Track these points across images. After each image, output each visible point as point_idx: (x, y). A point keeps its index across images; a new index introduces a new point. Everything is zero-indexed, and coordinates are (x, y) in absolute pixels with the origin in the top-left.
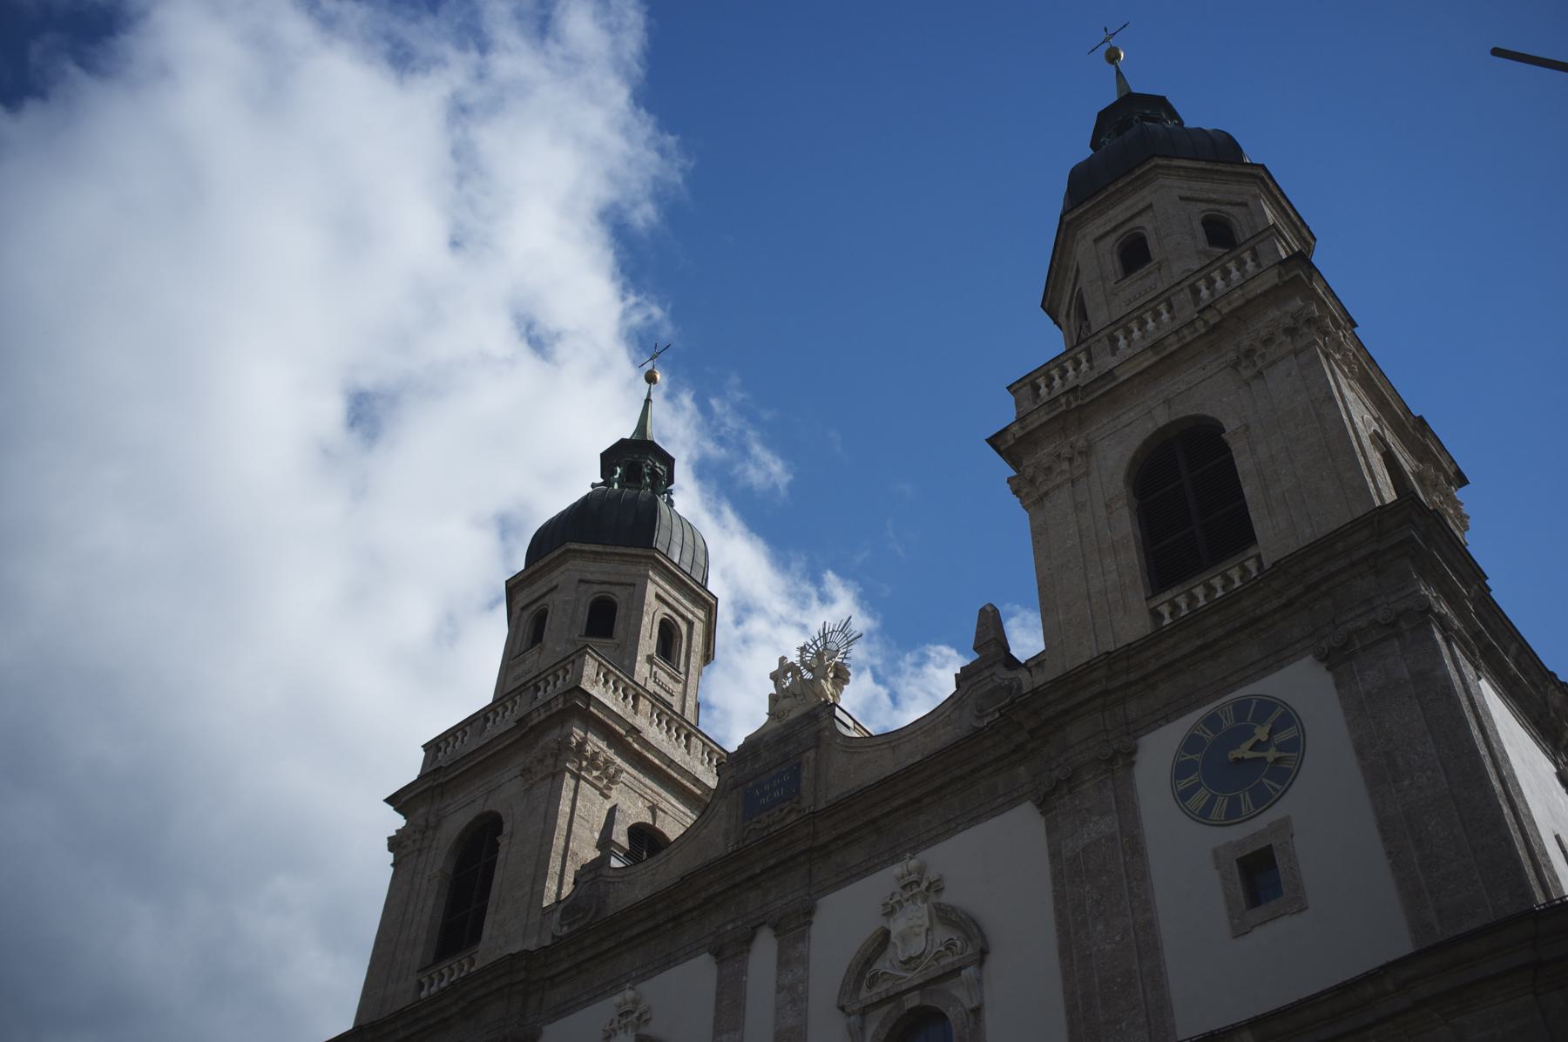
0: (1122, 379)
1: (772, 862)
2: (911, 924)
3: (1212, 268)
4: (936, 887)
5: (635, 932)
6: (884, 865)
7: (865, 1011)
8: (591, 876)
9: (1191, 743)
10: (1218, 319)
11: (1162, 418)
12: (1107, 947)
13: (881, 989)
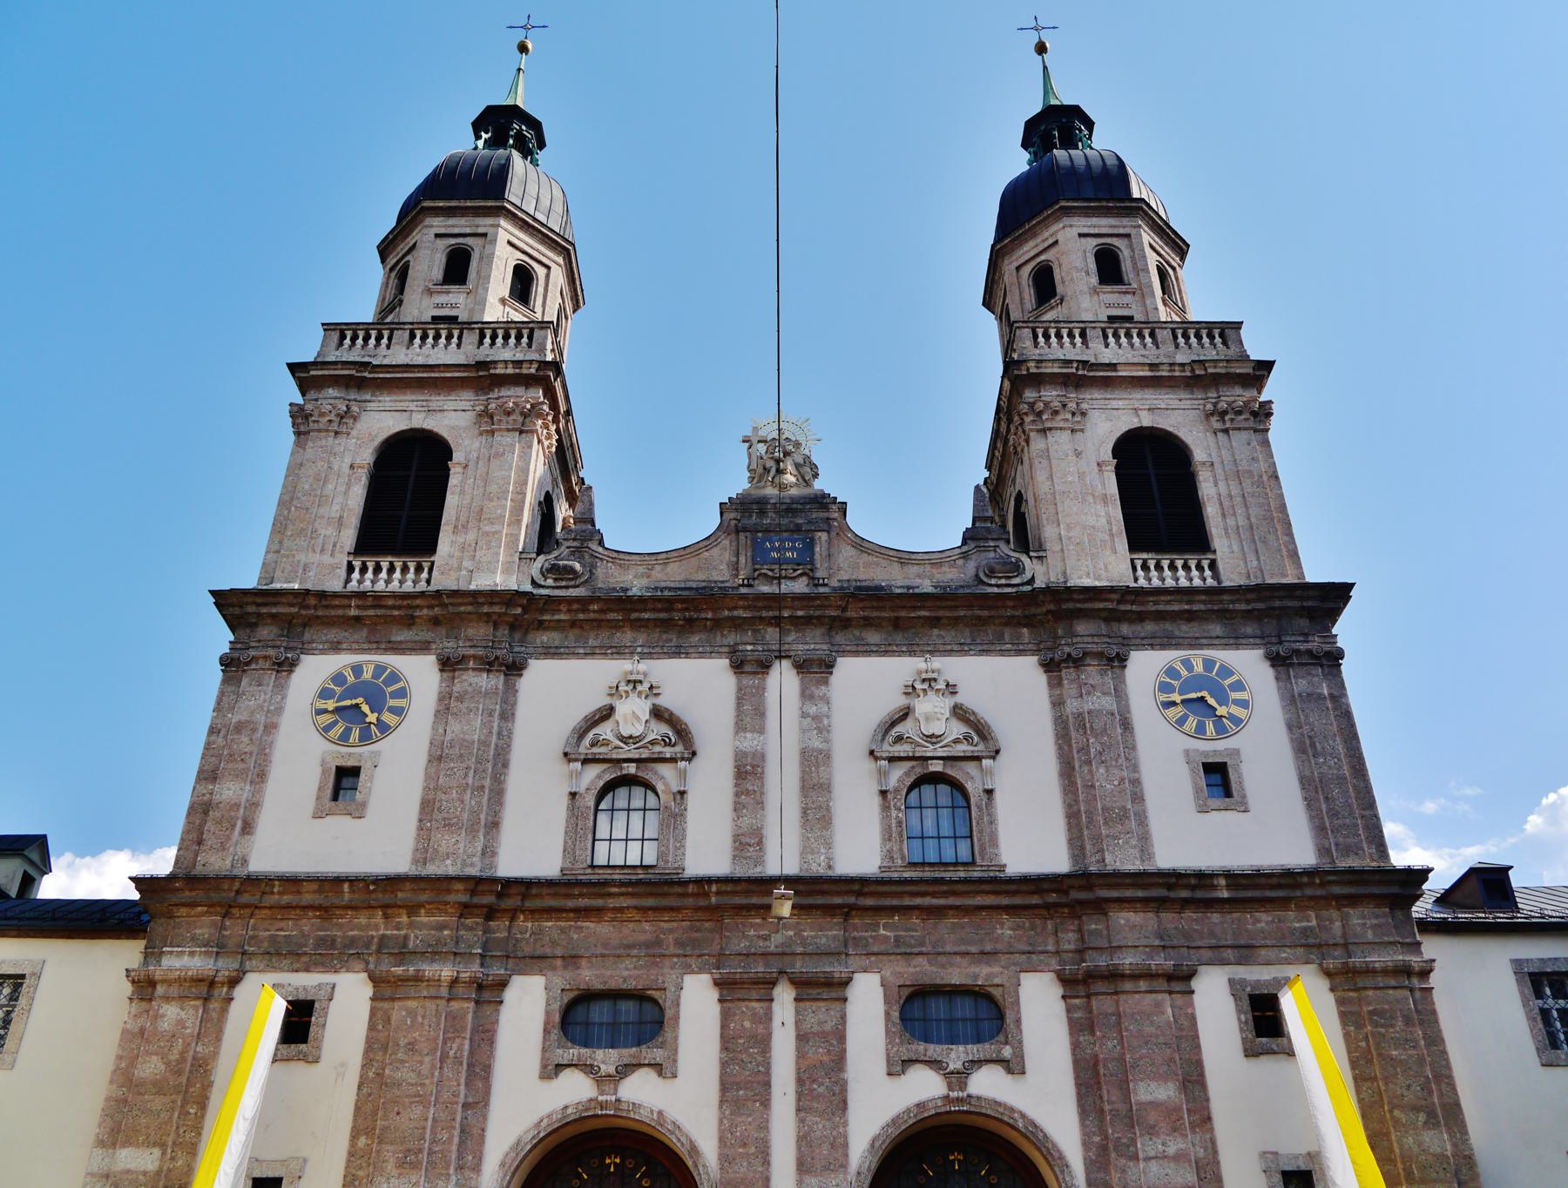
0: (1120, 374)
1: (800, 613)
2: (936, 710)
3: (1192, 326)
4: (951, 689)
5: (646, 616)
6: (901, 653)
7: (892, 760)
8: (576, 544)
9: (1171, 672)
10: (1203, 372)
11: (1147, 420)
12: (1108, 786)
13: (902, 749)
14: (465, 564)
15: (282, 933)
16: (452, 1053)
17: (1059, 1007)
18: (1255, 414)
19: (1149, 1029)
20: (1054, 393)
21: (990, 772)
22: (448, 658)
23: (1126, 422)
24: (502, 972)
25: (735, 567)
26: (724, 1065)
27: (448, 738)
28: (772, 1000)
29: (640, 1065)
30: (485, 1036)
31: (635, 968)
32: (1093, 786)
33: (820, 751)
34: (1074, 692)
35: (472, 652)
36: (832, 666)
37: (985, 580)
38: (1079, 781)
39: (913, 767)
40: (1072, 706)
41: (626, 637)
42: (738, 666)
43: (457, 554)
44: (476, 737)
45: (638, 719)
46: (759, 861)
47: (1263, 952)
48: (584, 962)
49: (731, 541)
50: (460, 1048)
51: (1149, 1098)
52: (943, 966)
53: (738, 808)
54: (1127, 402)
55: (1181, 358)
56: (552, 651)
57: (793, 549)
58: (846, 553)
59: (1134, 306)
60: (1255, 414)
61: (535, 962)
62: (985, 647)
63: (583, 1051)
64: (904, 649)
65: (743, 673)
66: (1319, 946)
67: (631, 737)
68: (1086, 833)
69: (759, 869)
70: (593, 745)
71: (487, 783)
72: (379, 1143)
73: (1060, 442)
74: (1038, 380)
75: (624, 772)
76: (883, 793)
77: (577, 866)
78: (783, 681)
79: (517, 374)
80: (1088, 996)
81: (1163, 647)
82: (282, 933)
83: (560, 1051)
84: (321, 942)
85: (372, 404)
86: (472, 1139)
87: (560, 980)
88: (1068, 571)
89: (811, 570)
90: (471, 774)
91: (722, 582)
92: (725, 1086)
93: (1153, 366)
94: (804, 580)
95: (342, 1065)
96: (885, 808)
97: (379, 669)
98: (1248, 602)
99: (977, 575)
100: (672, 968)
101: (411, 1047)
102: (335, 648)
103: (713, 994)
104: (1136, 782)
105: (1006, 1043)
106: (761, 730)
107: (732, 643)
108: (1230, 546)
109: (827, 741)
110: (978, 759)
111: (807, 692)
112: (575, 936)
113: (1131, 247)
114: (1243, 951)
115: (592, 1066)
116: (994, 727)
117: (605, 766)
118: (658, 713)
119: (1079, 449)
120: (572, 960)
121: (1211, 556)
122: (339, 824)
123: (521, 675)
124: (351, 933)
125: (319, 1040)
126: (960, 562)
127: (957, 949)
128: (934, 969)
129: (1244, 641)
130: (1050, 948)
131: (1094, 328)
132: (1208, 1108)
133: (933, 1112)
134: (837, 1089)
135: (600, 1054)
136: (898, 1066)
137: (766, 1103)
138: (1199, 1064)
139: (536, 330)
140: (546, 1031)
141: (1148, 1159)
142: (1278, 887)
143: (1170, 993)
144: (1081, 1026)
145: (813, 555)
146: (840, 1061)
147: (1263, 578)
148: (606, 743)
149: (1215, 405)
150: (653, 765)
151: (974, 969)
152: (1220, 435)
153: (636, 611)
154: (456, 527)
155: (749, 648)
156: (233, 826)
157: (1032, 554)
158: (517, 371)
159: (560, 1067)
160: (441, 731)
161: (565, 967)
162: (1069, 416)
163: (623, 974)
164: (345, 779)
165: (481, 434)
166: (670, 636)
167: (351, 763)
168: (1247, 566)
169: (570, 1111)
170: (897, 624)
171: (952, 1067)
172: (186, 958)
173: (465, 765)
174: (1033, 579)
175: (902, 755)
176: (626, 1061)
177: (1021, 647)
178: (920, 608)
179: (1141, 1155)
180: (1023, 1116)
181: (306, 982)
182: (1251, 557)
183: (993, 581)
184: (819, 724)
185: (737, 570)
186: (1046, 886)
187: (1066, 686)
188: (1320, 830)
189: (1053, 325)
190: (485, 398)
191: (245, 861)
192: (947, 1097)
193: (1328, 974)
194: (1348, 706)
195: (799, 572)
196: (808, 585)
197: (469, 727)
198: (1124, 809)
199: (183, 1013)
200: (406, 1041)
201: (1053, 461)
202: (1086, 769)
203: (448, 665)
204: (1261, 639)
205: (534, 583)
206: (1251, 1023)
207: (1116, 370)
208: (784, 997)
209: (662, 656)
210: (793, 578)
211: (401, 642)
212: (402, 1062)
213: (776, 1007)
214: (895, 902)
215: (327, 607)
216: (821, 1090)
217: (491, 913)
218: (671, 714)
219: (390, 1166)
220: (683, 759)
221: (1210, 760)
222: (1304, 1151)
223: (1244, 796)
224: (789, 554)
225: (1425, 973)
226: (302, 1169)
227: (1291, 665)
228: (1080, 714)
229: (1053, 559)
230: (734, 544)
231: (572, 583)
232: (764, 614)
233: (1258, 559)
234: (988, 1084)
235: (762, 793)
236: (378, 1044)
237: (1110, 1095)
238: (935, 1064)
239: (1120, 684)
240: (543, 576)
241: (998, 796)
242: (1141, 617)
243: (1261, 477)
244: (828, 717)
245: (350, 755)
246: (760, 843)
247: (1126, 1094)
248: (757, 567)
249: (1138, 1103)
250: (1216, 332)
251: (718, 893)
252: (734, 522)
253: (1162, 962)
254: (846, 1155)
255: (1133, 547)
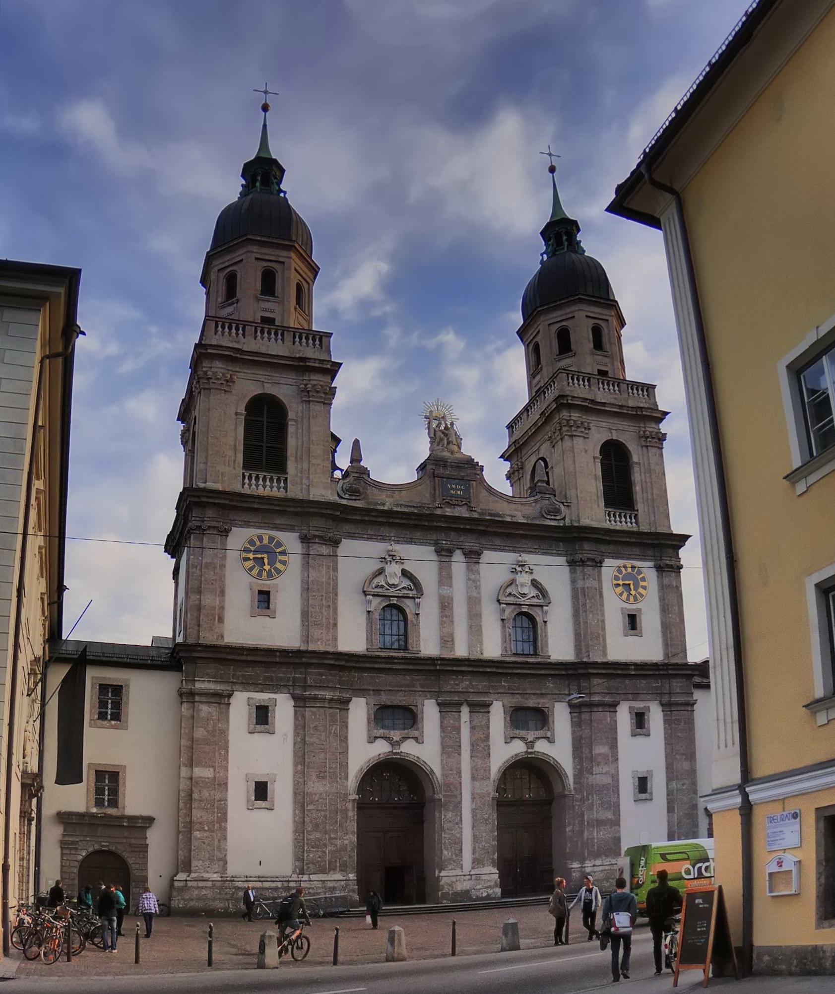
1: (468, 527)
2: (526, 581)
6: (509, 551)
13: (511, 600)
14: (304, 481)
15: (248, 674)
16: (333, 731)
17: (569, 716)
18: (659, 439)
19: (601, 726)
20: (577, 415)
21: (546, 613)
22: (306, 536)
23: (605, 437)
24: (348, 696)
25: (433, 496)
26: (443, 739)
27: (310, 579)
28: (460, 712)
29: (409, 738)
30: (345, 724)
31: (404, 696)
32: (587, 622)
33: (476, 598)
34: (581, 577)
35: (317, 533)
36: (479, 555)
37: (545, 516)
38: (581, 619)
39: (515, 609)
40: (580, 584)
41: (385, 531)
42: (438, 552)
43: (299, 474)
44: (324, 580)
45: (396, 575)
46: (452, 649)
47: (642, 696)
48: (382, 693)
49: (430, 481)
50: (336, 729)
51: (599, 752)
52: (526, 699)
53: (442, 623)
54: (607, 424)
55: (631, 403)
56: (353, 535)
57: (460, 490)
58: (484, 494)
59: (609, 365)
60: (659, 439)
61: (361, 692)
62: (545, 551)
63: (385, 731)
64: (511, 549)
65: (441, 555)
66: (661, 693)
67: (394, 585)
68: (583, 643)
69: (452, 653)
70: (377, 587)
71: (331, 604)
72: (308, 768)
73: (579, 442)
74: (570, 407)
75: (392, 602)
76: (503, 620)
77: (374, 647)
78: (458, 563)
79: (320, 367)
80: (580, 713)
81: (617, 558)
82: (248, 674)
83: (376, 731)
84: (266, 678)
85: (241, 374)
86: (344, 766)
87: (373, 700)
88: (580, 515)
89: (469, 502)
90: (324, 599)
91: (428, 504)
92: (444, 747)
93: (621, 407)
94: (465, 507)
95: (285, 735)
96: (504, 627)
97: (271, 539)
98: (652, 539)
99: (540, 512)
100: (419, 696)
101: (316, 728)
102: (247, 524)
103: (437, 709)
104: (603, 621)
105: (549, 730)
106: (451, 586)
107: (435, 539)
108: (644, 508)
109: (479, 593)
110: (542, 606)
111: (470, 568)
112: (377, 681)
113: (608, 326)
114: (635, 695)
115: (389, 738)
116: (549, 592)
117: (383, 598)
118: (405, 573)
119: (587, 448)
120: (377, 692)
121: (636, 513)
122: (263, 621)
123: (338, 547)
124: (279, 675)
125: (273, 723)
126: (534, 504)
127: (532, 692)
128: (522, 700)
129: (646, 558)
130: (567, 692)
131: (594, 378)
132: (617, 755)
133: (521, 757)
134: (486, 748)
135: (392, 732)
136: (509, 740)
137: (460, 754)
138: (616, 739)
139: (323, 337)
140: (369, 722)
141: (596, 774)
142: (651, 670)
143: (610, 711)
144: (576, 724)
145: (470, 493)
146: (487, 737)
147: (656, 528)
148: (382, 587)
149: (644, 432)
150: (403, 599)
151: (538, 700)
152: (644, 449)
153: (393, 518)
154: (296, 458)
155: (444, 542)
156: (215, 619)
157: (565, 504)
158: (321, 365)
159: (376, 738)
160: (306, 575)
161: (374, 695)
162: (583, 430)
163: (400, 699)
164: (264, 598)
165: (303, 401)
166: (406, 532)
167: (265, 589)
168: (650, 519)
169: (381, 756)
170: (508, 536)
171: (529, 740)
172: (206, 683)
173: (320, 594)
174: (564, 519)
175: (512, 602)
176: (403, 736)
177: (560, 552)
178: (521, 529)
179: (594, 773)
180: (553, 758)
181: (263, 697)
182: (652, 515)
183: (549, 517)
184: (474, 583)
185: (434, 498)
186: (569, 667)
187: (578, 574)
188: (666, 645)
189: (577, 373)
190: (301, 378)
191: (222, 637)
192: (527, 752)
193: (662, 705)
194: (681, 591)
195: (464, 503)
196: (467, 510)
197: (318, 574)
198: (598, 633)
199: (210, 709)
200: (313, 726)
201: (576, 454)
202: (584, 614)
203: (305, 540)
204: (654, 558)
205: (339, 495)
206: (635, 724)
207: (604, 406)
208: (465, 710)
209: (404, 542)
210: (460, 506)
211: (280, 524)
212: (312, 734)
213: (462, 714)
214: (510, 671)
215: (242, 502)
216: (481, 749)
217: (342, 668)
218: (412, 574)
219: (314, 778)
220: (417, 598)
221: (631, 613)
222: (645, 770)
223: (641, 630)
224: (459, 492)
225: (693, 705)
226: (275, 778)
227: (664, 571)
228: (583, 588)
229: (573, 507)
230: (432, 483)
231: (358, 498)
232: (452, 526)
233: (655, 516)
234: (541, 747)
235: (453, 617)
236: (300, 727)
237: (586, 751)
238: (522, 739)
239: (600, 573)
240: (344, 492)
241: (548, 623)
242: (609, 542)
243: (659, 474)
244: (480, 581)
245: (264, 584)
246: (453, 641)
247: (591, 750)
248: (444, 498)
249: (595, 754)
250: (645, 388)
251: (440, 665)
252: (432, 470)
253: (607, 699)
254: (490, 774)
255: (606, 505)
